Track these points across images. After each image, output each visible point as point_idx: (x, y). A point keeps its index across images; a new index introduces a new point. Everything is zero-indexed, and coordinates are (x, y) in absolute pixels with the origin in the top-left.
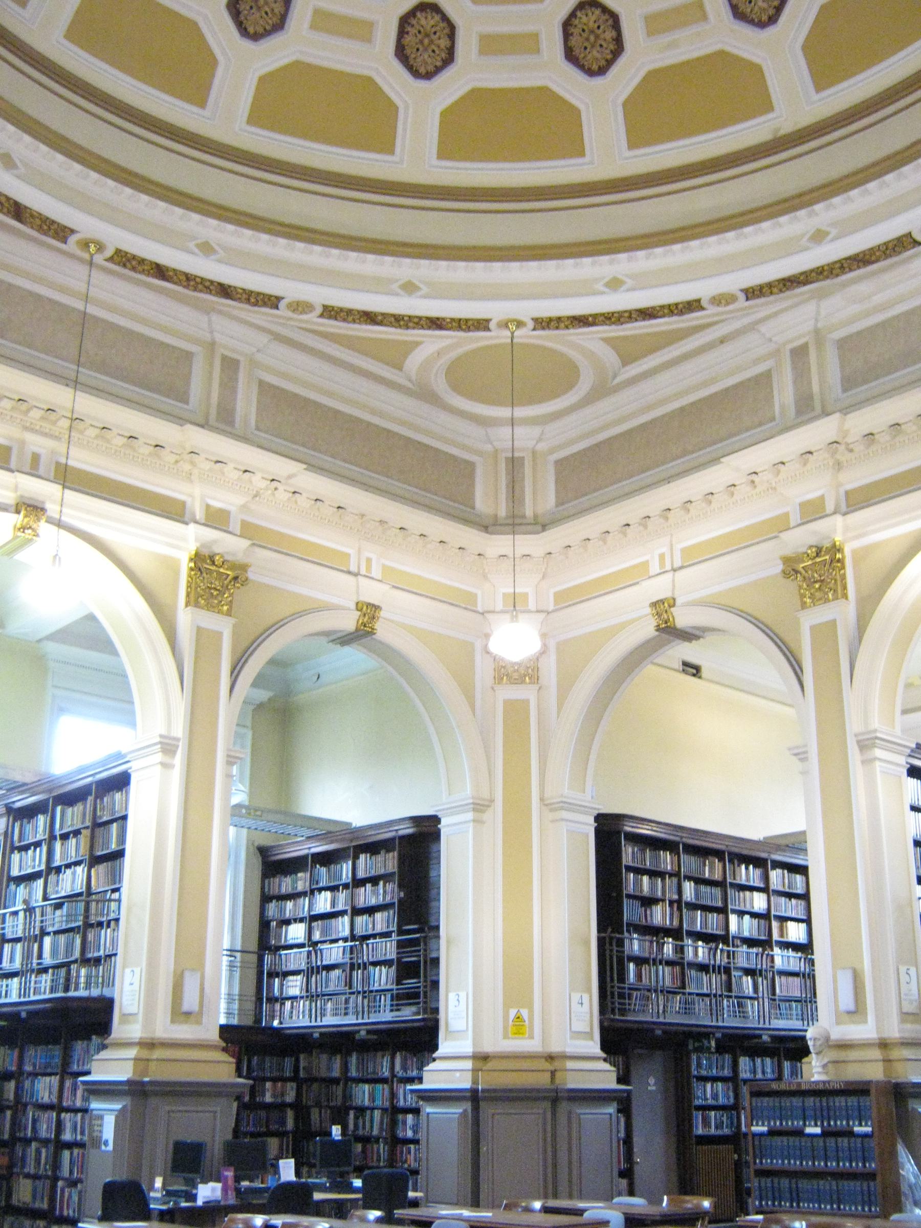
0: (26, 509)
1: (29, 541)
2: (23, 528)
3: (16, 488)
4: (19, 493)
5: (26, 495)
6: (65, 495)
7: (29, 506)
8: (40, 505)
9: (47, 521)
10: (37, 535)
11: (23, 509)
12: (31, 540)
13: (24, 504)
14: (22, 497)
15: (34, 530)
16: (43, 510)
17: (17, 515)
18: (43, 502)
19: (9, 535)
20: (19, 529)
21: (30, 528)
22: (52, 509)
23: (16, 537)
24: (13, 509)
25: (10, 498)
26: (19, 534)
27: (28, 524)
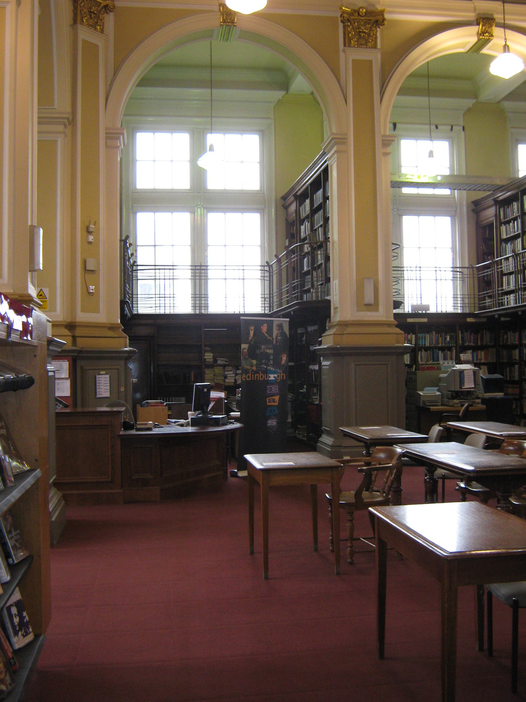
0: (483, 22)
1: (487, 41)
2: (483, 33)
3: (475, 10)
4: (477, 12)
5: (482, 12)
6: (505, 7)
7: (484, 19)
8: (491, 17)
9: (495, 26)
10: (492, 36)
11: (481, 21)
12: (489, 39)
13: (481, 18)
14: (479, 14)
15: (489, 33)
16: (493, 19)
17: (477, 27)
18: (492, 15)
19: (475, 39)
20: (481, 34)
21: (487, 32)
22: (498, 17)
23: (479, 40)
24: (475, 23)
25: (471, 16)
26: (481, 37)
27: (485, 30)
